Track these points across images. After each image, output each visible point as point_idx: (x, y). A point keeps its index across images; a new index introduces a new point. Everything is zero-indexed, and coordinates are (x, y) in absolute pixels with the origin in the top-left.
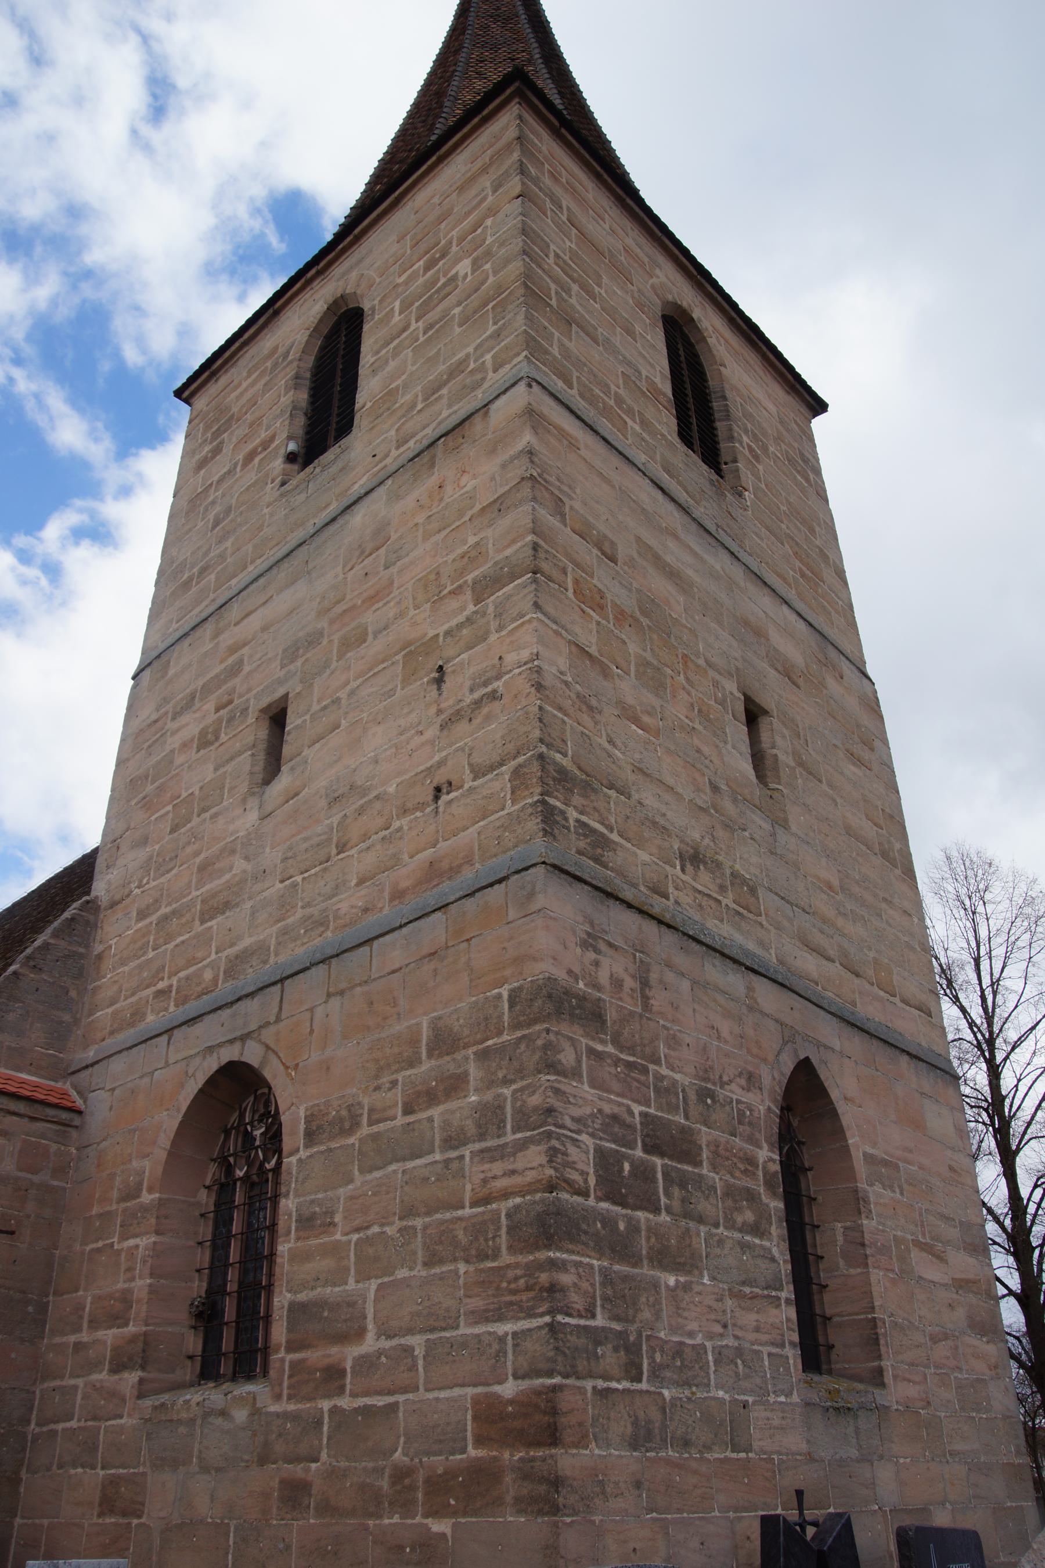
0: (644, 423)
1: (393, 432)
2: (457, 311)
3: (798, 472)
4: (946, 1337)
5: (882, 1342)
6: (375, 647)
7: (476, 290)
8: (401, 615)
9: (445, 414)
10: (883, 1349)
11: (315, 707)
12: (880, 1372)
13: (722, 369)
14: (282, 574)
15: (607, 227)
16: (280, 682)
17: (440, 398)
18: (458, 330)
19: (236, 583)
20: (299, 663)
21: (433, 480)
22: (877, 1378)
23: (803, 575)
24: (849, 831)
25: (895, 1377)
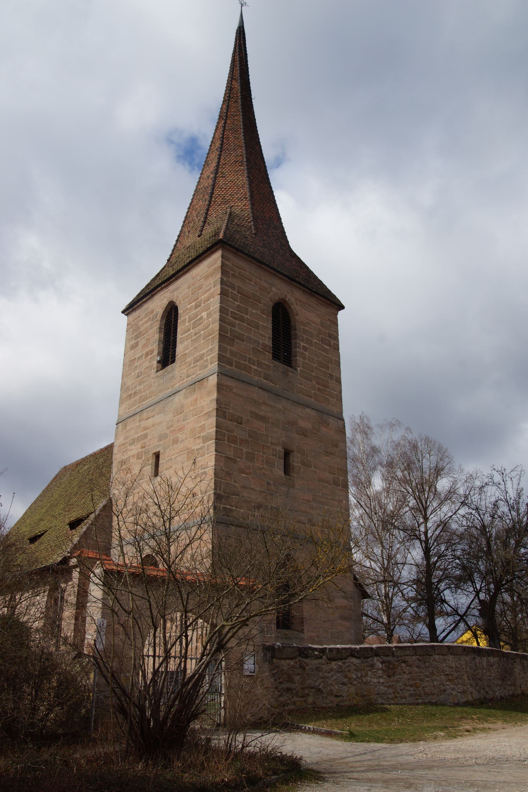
0: (259, 364)
1: (185, 371)
2: (202, 332)
3: (326, 344)
4: (329, 621)
5: (305, 622)
6: (180, 446)
7: (208, 328)
8: (186, 439)
9: (198, 372)
10: (304, 624)
11: (166, 459)
12: (303, 630)
13: (297, 317)
14: (158, 408)
15: (253, 283)
16: (158, 446)
17: (197, 365)
18: (203, 341)
19: (146, 403)
20: (162, 442)
21: (194, 397)
22: (302, 631)
23: (319, 390)
24: (320, 480)
25: (307, 631)
